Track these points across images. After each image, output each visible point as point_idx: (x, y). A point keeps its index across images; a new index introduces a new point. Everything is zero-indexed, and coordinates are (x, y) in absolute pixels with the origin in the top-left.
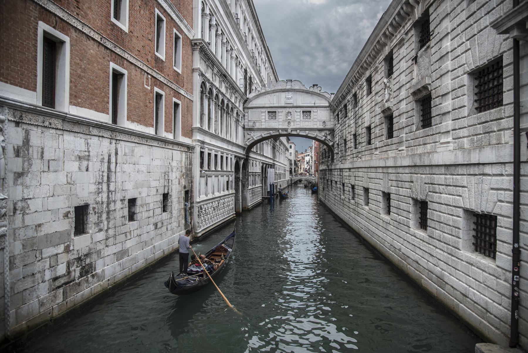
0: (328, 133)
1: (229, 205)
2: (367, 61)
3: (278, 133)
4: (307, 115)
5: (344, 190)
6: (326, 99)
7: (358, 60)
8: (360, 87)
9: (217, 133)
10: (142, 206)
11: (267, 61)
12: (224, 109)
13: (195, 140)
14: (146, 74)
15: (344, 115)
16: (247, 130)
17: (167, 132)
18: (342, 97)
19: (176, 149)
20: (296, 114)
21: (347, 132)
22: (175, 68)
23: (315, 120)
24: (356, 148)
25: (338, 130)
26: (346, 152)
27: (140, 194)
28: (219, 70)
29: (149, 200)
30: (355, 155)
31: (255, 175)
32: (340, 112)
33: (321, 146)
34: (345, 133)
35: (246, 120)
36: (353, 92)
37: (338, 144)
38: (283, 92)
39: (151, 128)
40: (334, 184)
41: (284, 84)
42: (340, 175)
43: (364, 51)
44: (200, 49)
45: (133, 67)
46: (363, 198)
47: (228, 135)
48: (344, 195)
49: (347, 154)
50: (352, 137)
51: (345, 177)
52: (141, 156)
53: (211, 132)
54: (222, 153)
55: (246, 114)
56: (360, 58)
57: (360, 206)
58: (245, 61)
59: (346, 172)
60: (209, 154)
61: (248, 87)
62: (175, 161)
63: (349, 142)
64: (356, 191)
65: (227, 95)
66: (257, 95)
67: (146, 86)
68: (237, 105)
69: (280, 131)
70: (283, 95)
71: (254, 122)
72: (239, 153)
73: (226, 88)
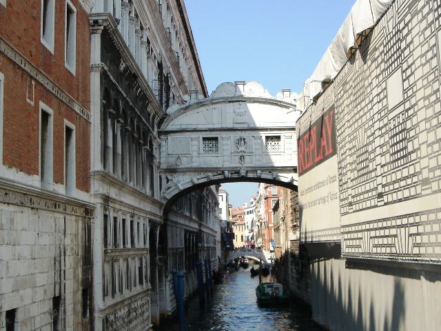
1: (143, 313)
3: (221, 177)
4: (273, 143)
9: (124, 178)
10: (24, 323)
12: (133, 137)
13: (95, 195)
14: (29, 79)
17: (57, 183)
19: (70, 213)
20: (254, 141)
22: (66, 65)
27: (22, 300)
29: (35, 310)
31: (176, 253)
35: (162, 155)
38: (230, 102)
39: (35, 176)
45: (11, 66)
52: (23, 230)
53: (116, 177)
54: (132, 216)
55: (163, 143)
58: (158, 48)
60: (115, 219)
62: (69, 236)
66: (182, 109)
67: (28, 100)
69: (226, 173)
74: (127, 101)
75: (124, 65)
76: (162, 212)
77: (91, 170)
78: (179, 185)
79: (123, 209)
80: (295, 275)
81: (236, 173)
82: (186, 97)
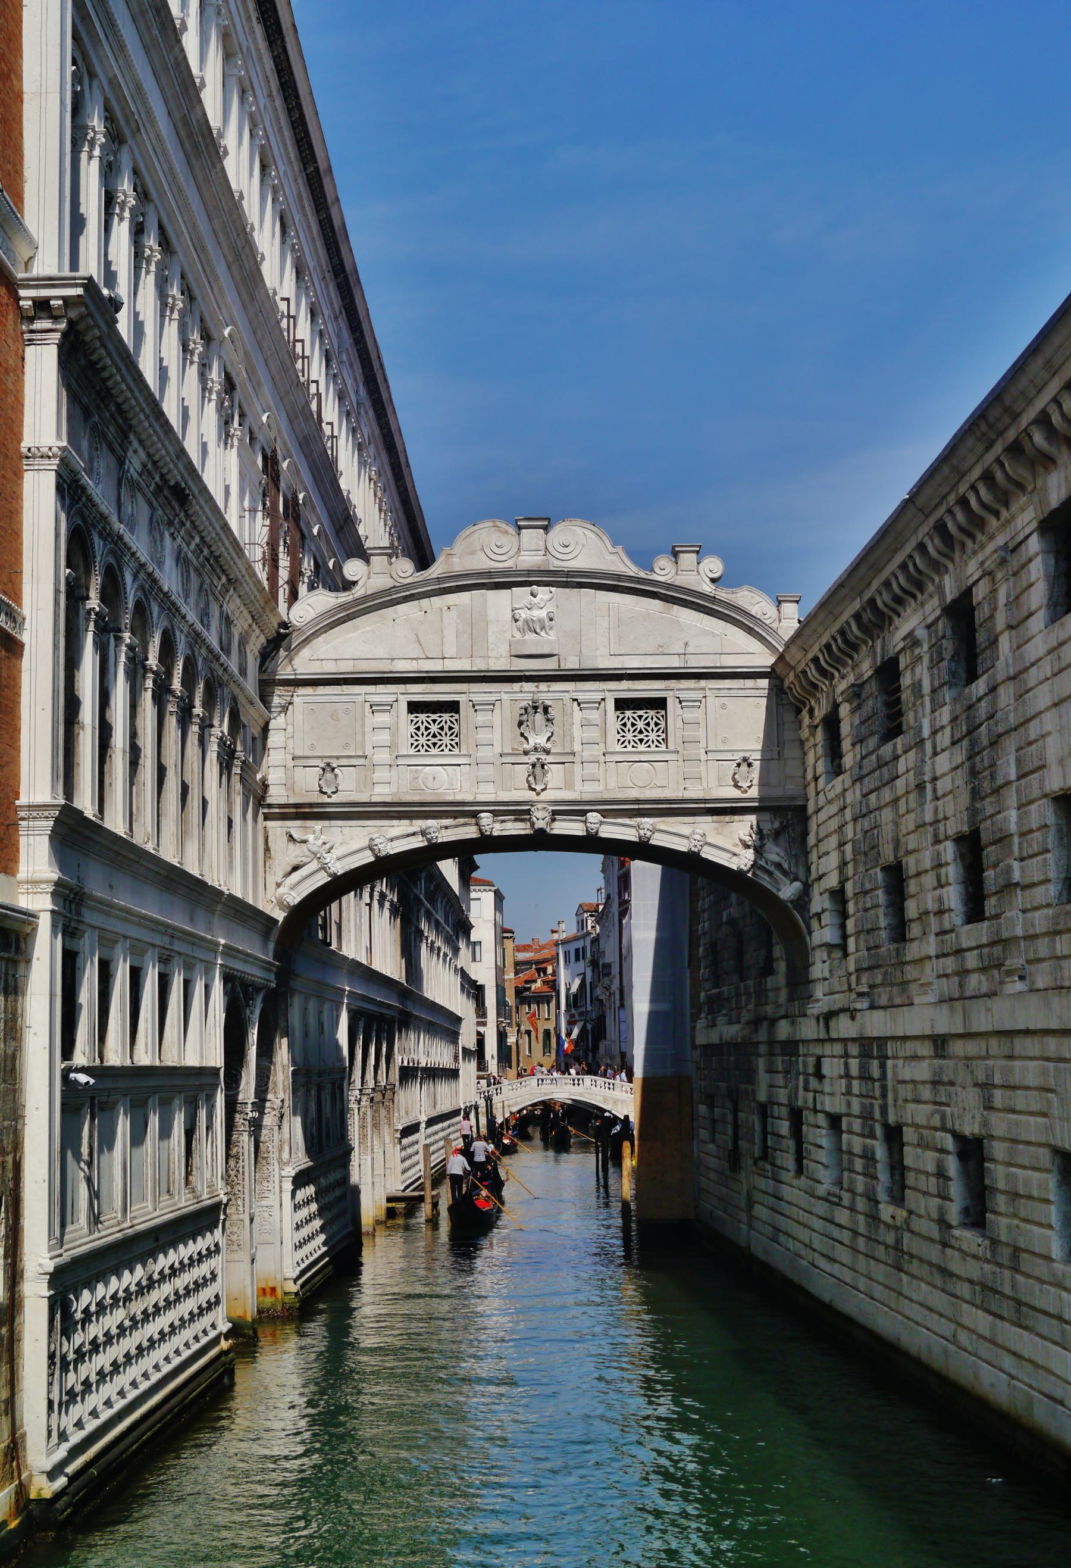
0: (767, 827)
2: (1056, 419)
3: (468, 832)
4: (640, 725)
5: (898, 1168)
6: (750, 631)
7: (995, 412)
8: (1003, 562)
11: (368, 403)
13: (35, 883)
15: (878, 724)
16: (284, 817)
18: (868, 616)
20: (577, 715)
21: (909, 822)
23: (691, 751)
24: (975, 912)
25: (833, 809)
26: (900, 932)
28: (153, 464)
30: (972, 960)
32: (844, 710)
33: (703, 904)
34: (887, 830)
36: (951, 591)
37: (838, 895)
40: (819, 1135)
41: (503, 540)
42: (865, 1076)
43: (1039, 361)
44: (65, 335)
46: (1054, 1214)
47: (192, 849)
48: (898, 1198)
49: (913, 951)
50: (949, 850)
51: (905, 1091)
54: (165, 960)
55: (277, 723)
56: (1007, 400)
57: (1040, 1269)
59: (915, 1057)
61: (281, 555)
63: (929, 880)
64: (999, 1175)
65: (184, 609)
68: (234, 666)
69: (486, 819)
70: (499, 601)
71: (329, 768)
72: (247, 957)
73: (181, 559)
74: (150, 575)
75: (143, 455)
76: (271, 946)
77: (23, 800)
78: (328, 858)
79: (133, 931)
80: (713, 1162)
81: (516, 820)
82: (353, 569)
